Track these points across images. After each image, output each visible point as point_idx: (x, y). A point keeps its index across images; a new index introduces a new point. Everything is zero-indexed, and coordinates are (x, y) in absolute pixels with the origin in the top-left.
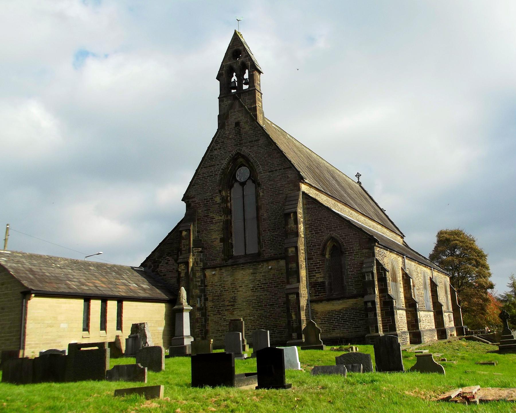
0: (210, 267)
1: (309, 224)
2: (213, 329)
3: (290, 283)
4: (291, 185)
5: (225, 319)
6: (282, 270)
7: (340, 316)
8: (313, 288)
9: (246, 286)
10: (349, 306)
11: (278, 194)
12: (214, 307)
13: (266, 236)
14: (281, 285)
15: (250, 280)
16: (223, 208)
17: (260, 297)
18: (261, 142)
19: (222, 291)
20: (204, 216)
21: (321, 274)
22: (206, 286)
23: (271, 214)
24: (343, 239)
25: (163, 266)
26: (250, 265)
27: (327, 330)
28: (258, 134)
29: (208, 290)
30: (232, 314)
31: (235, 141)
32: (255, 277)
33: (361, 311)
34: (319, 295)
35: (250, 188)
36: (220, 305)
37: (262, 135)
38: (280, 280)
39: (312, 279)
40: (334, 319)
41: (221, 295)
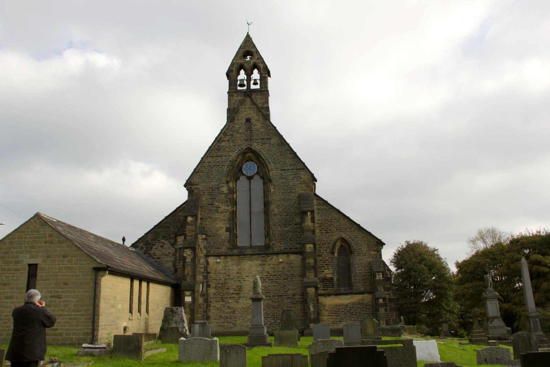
0: (215, 255)
1: (320, 223)
2: (215, 316)
4: (304, 185)
5: (229, 307)
6: (292, 264)
7: (347, 310)
8: (321, 283)
9: (254, 276)
10: (356, 301)
12: (217, 294)
13: (277, 230)
14: (291, 278)
15: (258, 271)
16: (230, 198)
17: (268, 288)
18: (273, 141)
19: (225, 279)
20: (208, 204)
21: (330, 271)
22: (209, 273)
23: (282, 210)
25: (157, 248)
26: (258, 257)
27: (334, 322)
28: (271, 133)
29: (210, 277)
30: (237, 302)
32: (263, 269)
33: (368, 306)
34: (327, 290)
35: (257, 183)
36: (224, 292)
38: (289, 273)
39: (320, 274)
40: (341, 312)
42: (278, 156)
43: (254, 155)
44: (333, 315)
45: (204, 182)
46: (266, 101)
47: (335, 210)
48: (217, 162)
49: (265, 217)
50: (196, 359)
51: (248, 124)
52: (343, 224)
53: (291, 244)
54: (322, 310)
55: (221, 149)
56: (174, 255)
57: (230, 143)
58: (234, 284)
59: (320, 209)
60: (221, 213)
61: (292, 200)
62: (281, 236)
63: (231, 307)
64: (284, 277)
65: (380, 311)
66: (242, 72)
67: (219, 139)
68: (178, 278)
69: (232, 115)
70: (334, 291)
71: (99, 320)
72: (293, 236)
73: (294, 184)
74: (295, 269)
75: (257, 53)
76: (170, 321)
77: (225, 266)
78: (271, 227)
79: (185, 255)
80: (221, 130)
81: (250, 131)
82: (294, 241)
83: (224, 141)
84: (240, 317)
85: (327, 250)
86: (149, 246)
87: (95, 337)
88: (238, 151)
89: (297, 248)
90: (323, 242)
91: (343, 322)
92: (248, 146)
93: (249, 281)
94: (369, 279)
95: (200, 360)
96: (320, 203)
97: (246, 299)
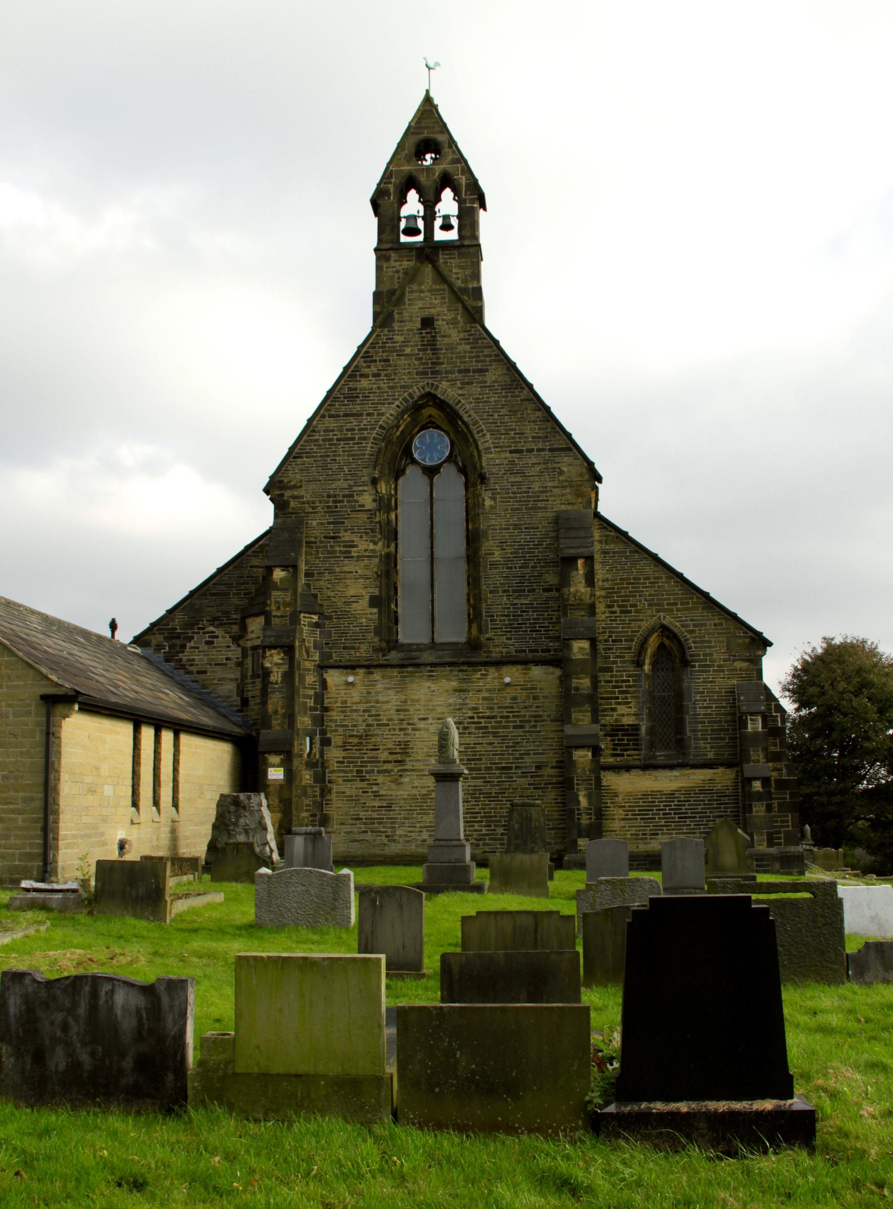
0: (342, 664)
2: (342, 815)
3: (574, 721)
4: (568, 490)
5: (376, 795)
6: (536, 689)
7: (671, 806)
8: (609, 738)
9: (439, 719)
11: (532, 508)
12: (348, 762)
13: (499, 605)
14: (533, 724)
15: (450, 705)
16: (380, 522)
17: (475, 748)
18: (490, 377)
19: (368, 725)
20: (325, 537)
21: (630, 707)
22: (326, 709)
23: (511, 553)
24: (691, 632)
25: (198, 648)
26: (451, 671)
27: (639, 835)
28: (486, 356)
29: (331, 720)
30: (397, 782)
31: (420, 364)
32: (463, 701)
33: (723, 798)
34: (623, 755)
36: (364, 758)
37: (494, 361)
38: (528, 711)
39: (606, 715)
41: (366, 736)
42: (504, 415)
43: (443, 413)
44: (637, 819)
45: (315, 481)
46: (473, 272)
47: (646, 556)
48: (348, 430)
49: (469, 570)
50: (298, 919)
51: (426, 333)
52: (667, 591)
53: (535, 638)
54: (609, 805)
55: (358, 397)
56: (239, 664)
57: (379, 380)
58: (390, 736)
59: (608, 553)
60: (357, 561)
61: (538, 528)
62: (509, 620)
63: (383, 795)
64: (515, 722)
65: (754, 809)
66: (413, 196)
67: (352, 371)
68: (251, 722)
69: (385, 310)
70: (639, 759)
71: (58, 823)
72: (539, 619)
73: (544, 487)
74: (543, 703)
75: (452, 147)
76: (231, 828)
77: (369, 693)
78: (483, 597)
79: (268, 665)
80: (359, 348)
81: (431, 350)
82: (541, 631)
83: (366, 376)
84: (405, 818)
85: (624, 657)
86: (178, 642)
87: (51, 863)
88: (401, 403)
89: (548, 651)
90: (616, 636)
91: (659, 837)
92: (427, 389)
93: (427, 730)
94: (728, 730)
95: (309, 922)
96: (610, 536)
97: (420, 775)
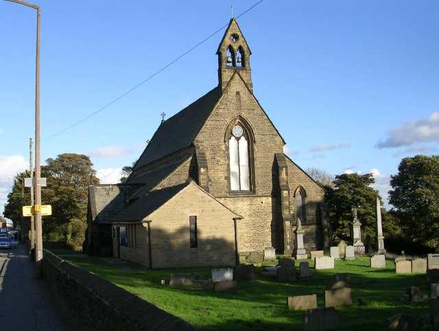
35: (244, 143)
